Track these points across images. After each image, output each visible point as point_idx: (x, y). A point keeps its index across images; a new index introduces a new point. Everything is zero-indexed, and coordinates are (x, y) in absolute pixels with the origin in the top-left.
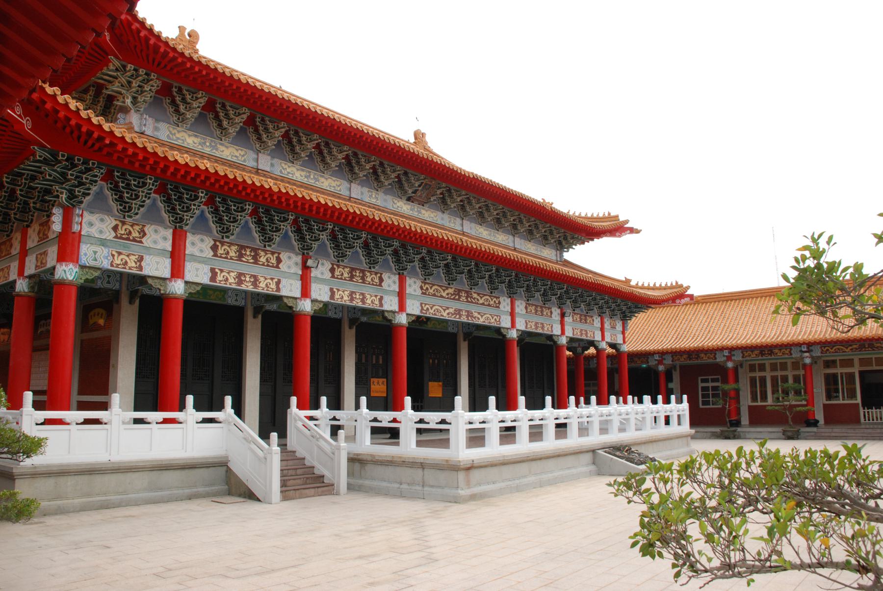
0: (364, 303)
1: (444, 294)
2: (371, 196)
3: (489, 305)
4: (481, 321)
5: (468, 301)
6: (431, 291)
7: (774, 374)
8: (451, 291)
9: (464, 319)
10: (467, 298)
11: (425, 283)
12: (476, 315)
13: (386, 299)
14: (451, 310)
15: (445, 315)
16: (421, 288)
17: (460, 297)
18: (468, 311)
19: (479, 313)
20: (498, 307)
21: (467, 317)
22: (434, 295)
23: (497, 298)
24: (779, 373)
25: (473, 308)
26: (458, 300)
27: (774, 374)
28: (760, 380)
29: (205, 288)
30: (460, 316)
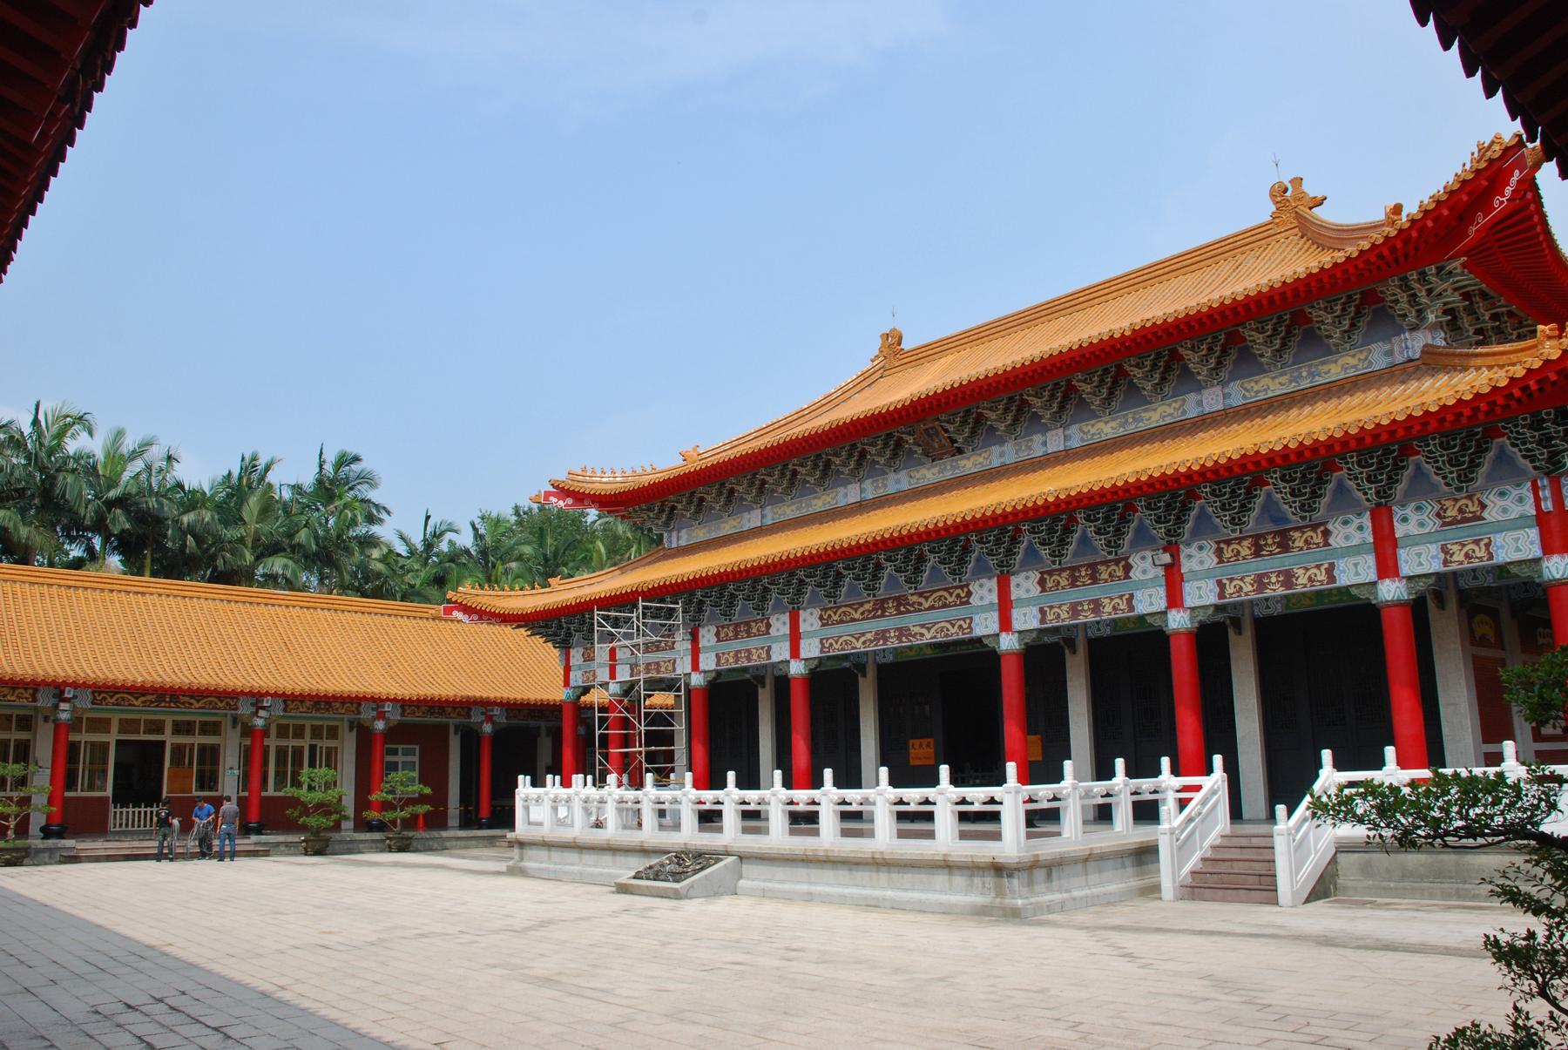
0: (749, 660)
1: (857, 616)
2: (876, 488)
3: (945, 606)
4: (928, 637)
5: (901, 613)
6: (835, 618)
7: (283, 743)
8: (867, 606)
9: (893, 643)
10: (897, 608)
11: (826, 610)
12: (917, 629)
13: (775, 648)
14: (869, 636)
15: (859, 647)
16: (821, 618)
17: (884, 610)
18: (900, 629)
19: (922, 626)
20: (968, 603)
21: (899, 639)
22: (841, 622)
23: (961, 587)
24: (292, 743)
25: (911, 621)
26: (882, 616)
27: (283, 743)
28: (294, 753)
29: (719, 673)
30: (886, 640)
